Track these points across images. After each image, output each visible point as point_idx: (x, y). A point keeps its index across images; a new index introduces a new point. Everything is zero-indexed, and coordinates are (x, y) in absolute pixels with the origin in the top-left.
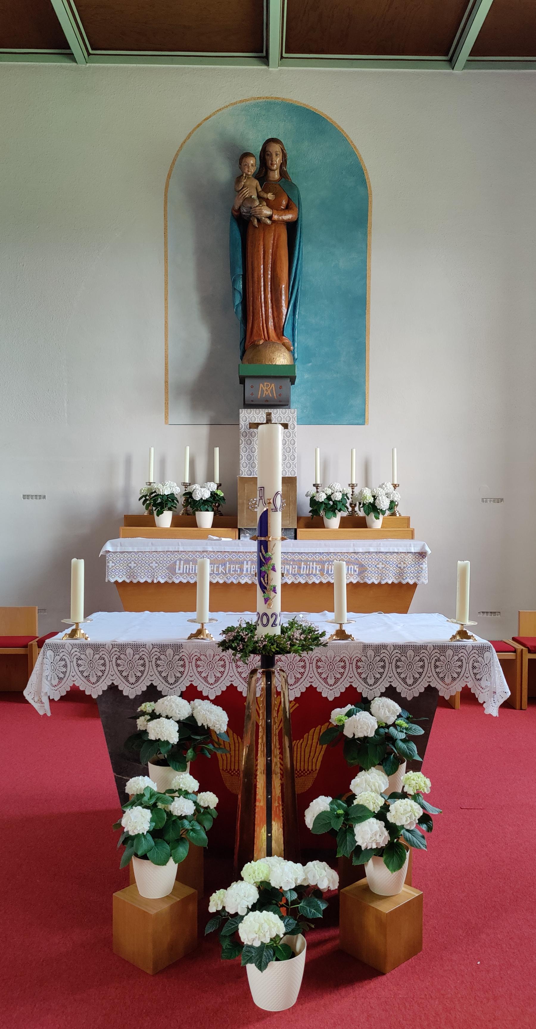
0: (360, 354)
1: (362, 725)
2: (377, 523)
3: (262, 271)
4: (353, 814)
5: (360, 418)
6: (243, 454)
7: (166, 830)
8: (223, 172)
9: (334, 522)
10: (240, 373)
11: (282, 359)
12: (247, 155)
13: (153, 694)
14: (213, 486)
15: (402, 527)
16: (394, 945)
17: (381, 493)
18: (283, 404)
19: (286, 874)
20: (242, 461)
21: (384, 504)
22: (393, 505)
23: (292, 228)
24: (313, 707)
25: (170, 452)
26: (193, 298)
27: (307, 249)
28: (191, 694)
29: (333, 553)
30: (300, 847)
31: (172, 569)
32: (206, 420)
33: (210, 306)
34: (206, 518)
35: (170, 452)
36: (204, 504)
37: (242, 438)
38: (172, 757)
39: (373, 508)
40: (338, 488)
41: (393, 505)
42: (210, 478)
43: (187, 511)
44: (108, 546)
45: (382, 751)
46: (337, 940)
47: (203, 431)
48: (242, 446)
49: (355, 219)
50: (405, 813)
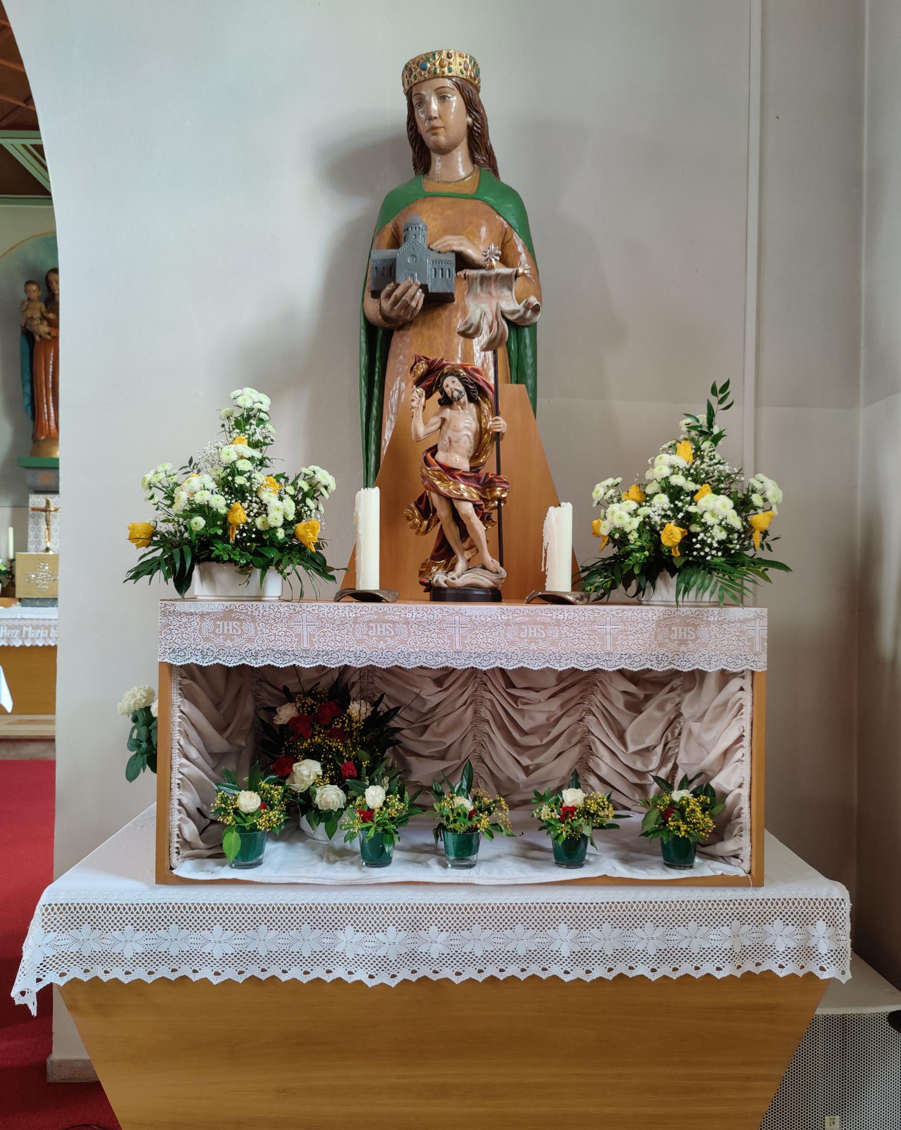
6: (31, 534)
20: (30, 540)
32: (8, 503)
37: (31, 520)
48: (30, 526)
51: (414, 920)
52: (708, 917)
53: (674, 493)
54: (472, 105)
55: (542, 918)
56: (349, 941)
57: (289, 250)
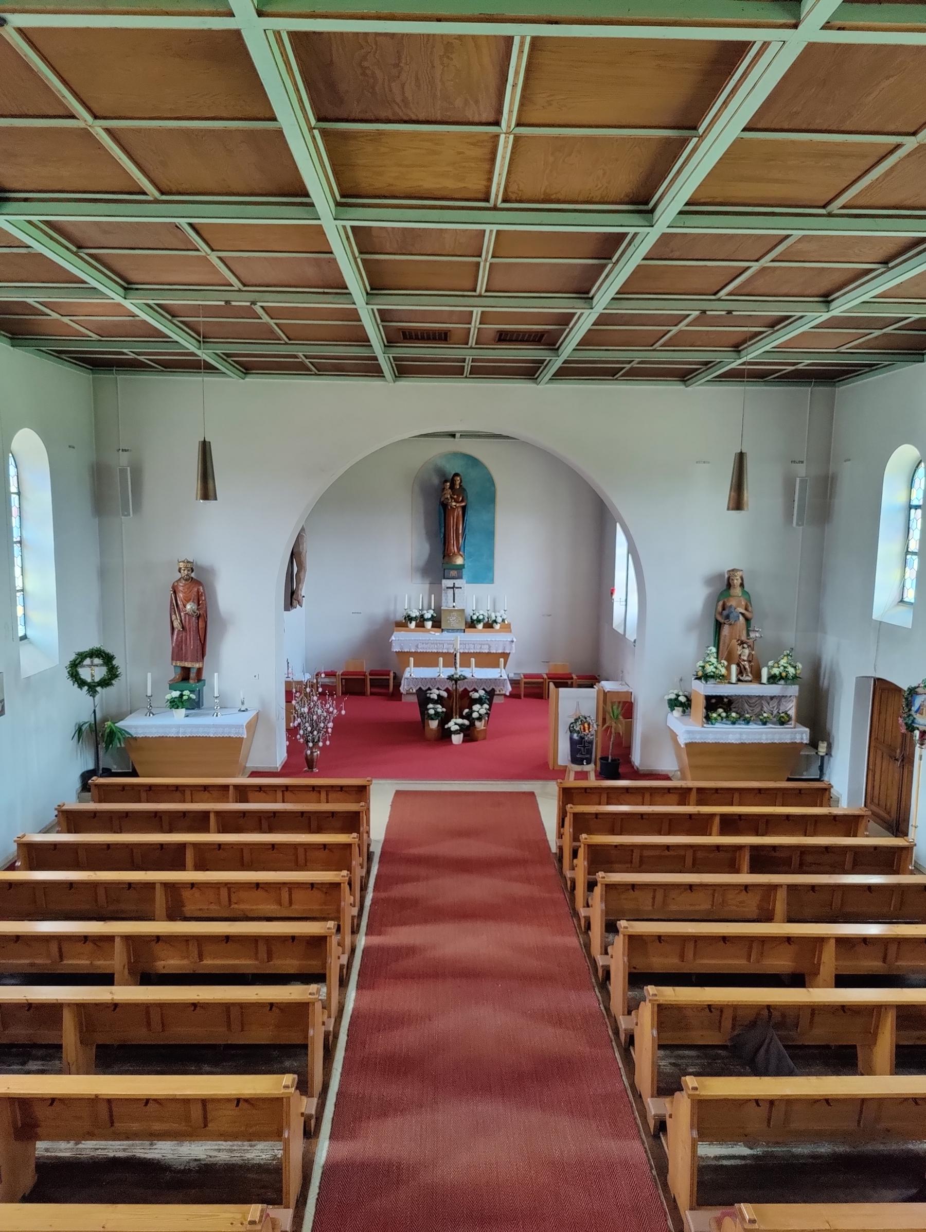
0: (492, 556)
1: (476, 695)
2: (497, 627)
3: (452, 522)
4: (472, 712)
6: (443, 598)
7: (437, 713)
8: (436, 481)
9: (480, 626)
10: (441, 563)
11: (459, 561)
12: (446, 481)
13: (429, 689)
14: (432, 612)
15: (507, 628)
16: (480, 736)
17: (498, 614)
18: (460, 577)
19: (460, 721)
21: (499, 620)
22: (503, 620)
23: (464, 508)
24: (466, 692)
25: (412, 596)
26: (423, 531)
27: (469, 512)
28: (438, 689)
29: (479, 640)
30: (462, 717)
31: (417, 646)
33: (430, 535)
34: (429, 624)
35: (412, 596)
36: (428, 620)
38: (435, 702)
39: (495, 621)
40: (482, 613)
41: (503, 620)
42: (430, 608)
43: (421, 622)
44: (393, 638)
45: (480, 701)
46: (469, 732)
47: (427, 586)
50: (483, 711)
51: (741, 734)
52: (787, 733)
53: (785, 667)
54: (742, 579)
55: (762, 733)
56: (731, 736)
57: (695, 599)
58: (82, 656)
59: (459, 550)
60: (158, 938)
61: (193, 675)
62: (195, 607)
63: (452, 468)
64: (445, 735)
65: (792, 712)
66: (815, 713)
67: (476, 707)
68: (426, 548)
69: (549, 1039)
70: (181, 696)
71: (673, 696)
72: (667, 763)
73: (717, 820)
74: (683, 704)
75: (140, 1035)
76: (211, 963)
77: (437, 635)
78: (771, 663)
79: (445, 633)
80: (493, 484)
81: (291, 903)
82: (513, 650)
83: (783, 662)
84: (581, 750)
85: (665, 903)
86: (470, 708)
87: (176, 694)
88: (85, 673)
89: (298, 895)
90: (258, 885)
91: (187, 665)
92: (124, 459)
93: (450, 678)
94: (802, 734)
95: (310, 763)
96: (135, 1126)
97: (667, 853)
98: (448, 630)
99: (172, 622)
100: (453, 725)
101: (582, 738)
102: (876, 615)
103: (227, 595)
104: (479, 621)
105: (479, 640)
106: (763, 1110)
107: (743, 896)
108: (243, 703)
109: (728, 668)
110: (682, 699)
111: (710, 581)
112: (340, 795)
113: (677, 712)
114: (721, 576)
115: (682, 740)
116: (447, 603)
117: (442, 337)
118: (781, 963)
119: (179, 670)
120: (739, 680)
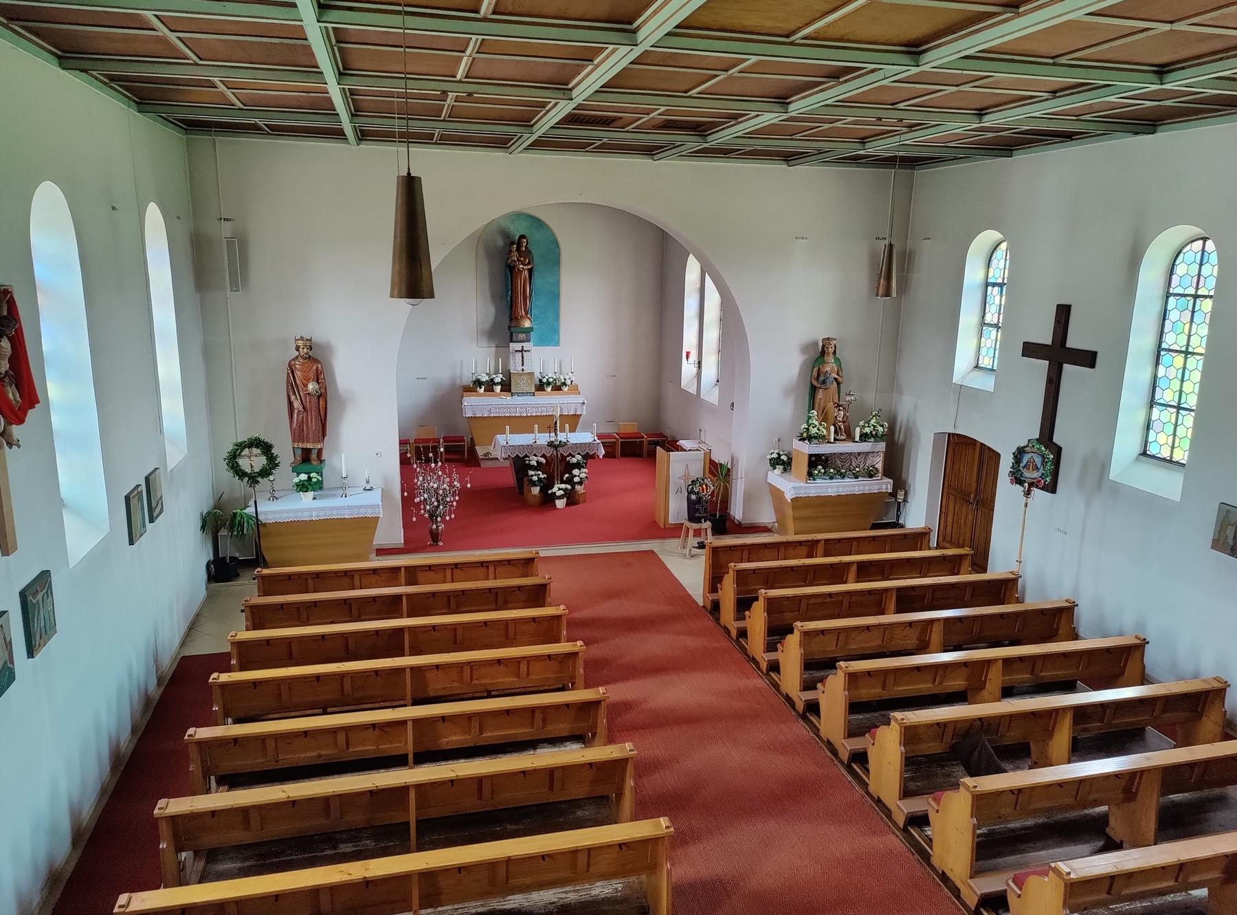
1: (574, 460)
2: (566, 389)
5: (558, 344)
7: (539, 479)
9: (549, 389)
11: (527, 324)
12: (513, 243)
15: (575, 390)
18: (528, 341)
19: (563, 486)
21: (568, 382)
23: (530, 271)
25: (478, 359)
26: (488, 294)
27: (536, 274)
29: (550, 403)
33: (496, 298)
34: (498, 389)
35: (478, 359)
39: (564, 384)
40: (550, 375)
42: (496, 372)
43: (490, 386)
45: (578, 465)
46: (571, 498)
49: (557, 262)
58: (241, 446)
59: (527, 313)
60: (443, 718)
61: (314, 456)
62: (317, 387)
63: (516, 230)
64: (548, 500)
65: (880, 466)
66: (895, 466)
67: (576, 472)
68: (491, 312)
69: (781, 766)
70: (310, 478)
71: (775, 456)
72: (766, 516)
73: (854, 568)
74: (783, 463)
75: (471, 805)
76: (492, 735)
77: (507, 399)
78: (861, 423)
79: (516, 397)
80: (558, 246)
81: (528, 675)
82: (583, 411)
83: (873, 422)
84: (696, 510)
85: (846, 643)
86: (570, 473)
87: (304, 477)
88: (244, 464)
89: (535, 666)
90: (499, 661)
91: (309, 446)
92: (226, 229)
93: (551, 444)
94: (886, 485)
95: (435, 536)
96: (528, 880)
97: (829, 599)
98: (518, 394)
99: (290, 404)
100: (558, 489)
101: (699, 500)
102: (957, 378)
103: (347, 372)
104: (548, 383)
105: (550, 403)
106: (1012, 798)
107: (908, 631)
108: (368, 482)
109: (828, 430)
110: (784, 458)
111: (805, 349)
112: (507, 569)
113: (779, 469)
114: (815, 344)
115: (789, 496)
116: (515, 366)
117: (606, 122)
118: (956, 683)
119: (299, 452)
120: (835, 439)
